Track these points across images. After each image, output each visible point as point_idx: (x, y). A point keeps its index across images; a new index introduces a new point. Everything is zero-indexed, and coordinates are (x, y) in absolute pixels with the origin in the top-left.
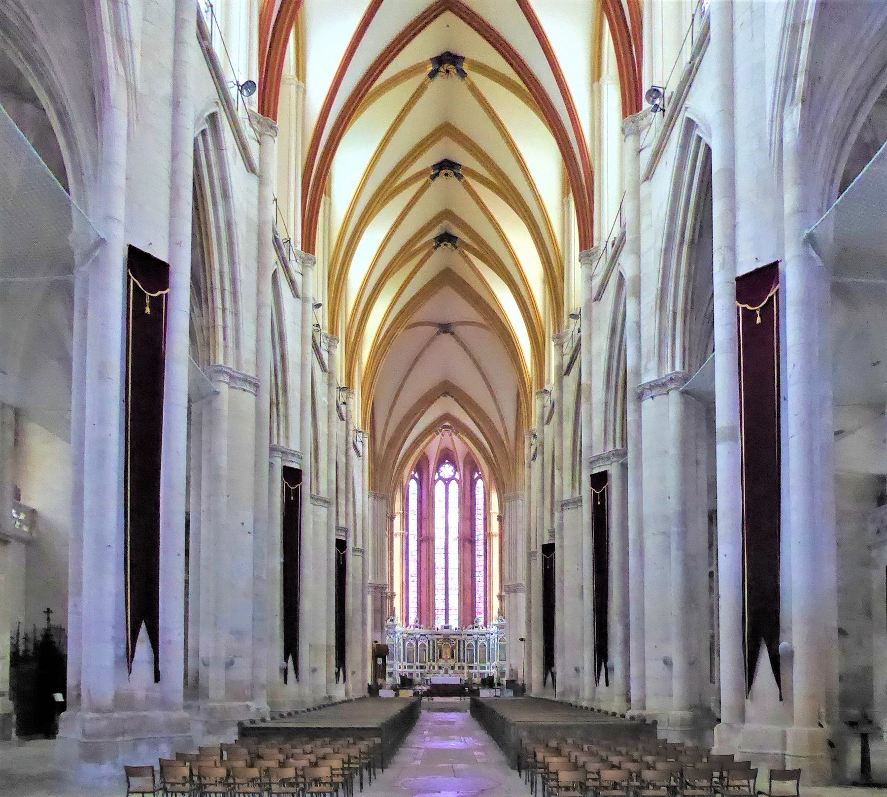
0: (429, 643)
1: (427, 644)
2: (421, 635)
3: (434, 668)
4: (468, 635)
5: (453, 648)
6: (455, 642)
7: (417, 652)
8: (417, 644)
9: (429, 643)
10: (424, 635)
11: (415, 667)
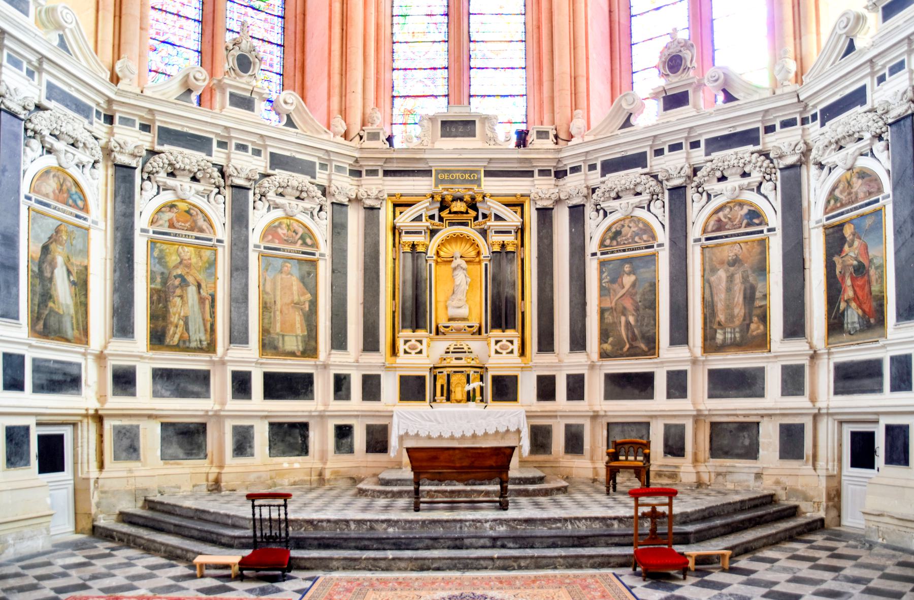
0: (339, 229)
1: (321, 229)
2: (277, 161)
3: (371, 388)
4: (610, 167)
5: (502, 254)
6: (512, 219)
7: (239, 268)
8: (239, 219)
9: (339, 229)
10: (307, 168)
11: (221, 383)
